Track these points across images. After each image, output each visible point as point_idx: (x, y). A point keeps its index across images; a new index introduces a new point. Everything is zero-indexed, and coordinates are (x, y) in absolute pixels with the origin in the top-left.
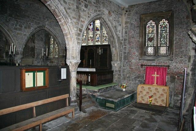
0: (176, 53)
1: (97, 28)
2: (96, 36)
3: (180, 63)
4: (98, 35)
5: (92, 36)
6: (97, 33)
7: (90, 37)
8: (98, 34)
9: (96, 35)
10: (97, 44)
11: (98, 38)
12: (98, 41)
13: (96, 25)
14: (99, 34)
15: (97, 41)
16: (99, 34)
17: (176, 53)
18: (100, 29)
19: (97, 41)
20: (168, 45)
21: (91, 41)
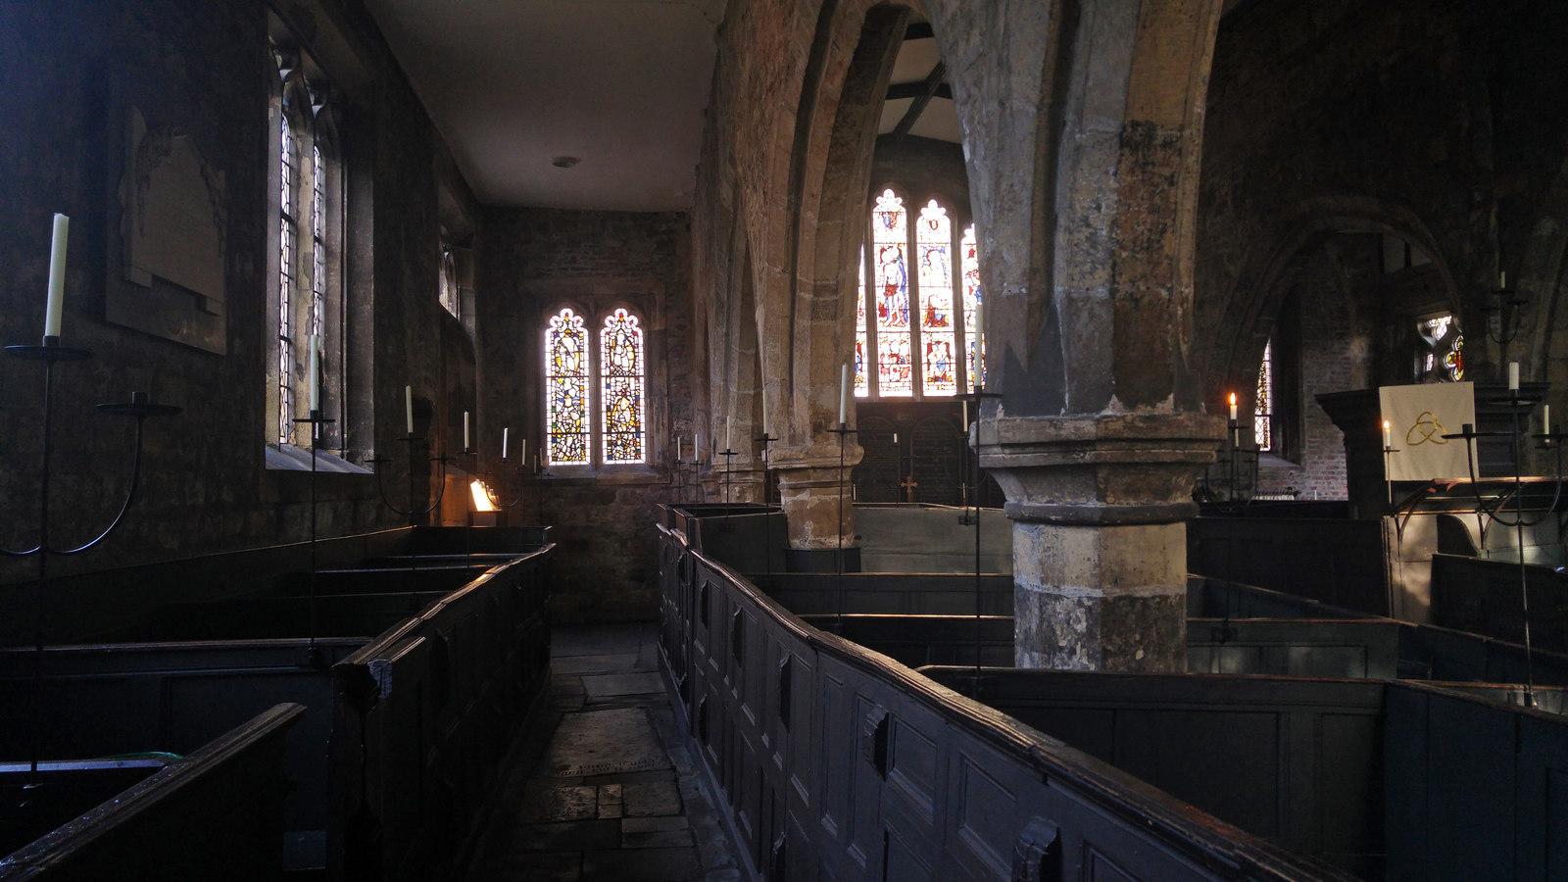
0: (1313, 442)
1: (931, 311)
2: (930, 350)
3: (1327, 478)
4: (942, 347)
5: (905, 350)
6: (936, 337)
7: (892, 355)
8: (938, 343)
9: (930, 346)
10: (931, 391)
11: (939, 364)
12: (944, 378)
13: (923, 294)
14: (947, 344)
15: (936, 379)
16: (947, 344)
17: (1313, 442)
18: (950, 319)
19: (936, 379)
20: (1268, 412)
21: (896, 376)
